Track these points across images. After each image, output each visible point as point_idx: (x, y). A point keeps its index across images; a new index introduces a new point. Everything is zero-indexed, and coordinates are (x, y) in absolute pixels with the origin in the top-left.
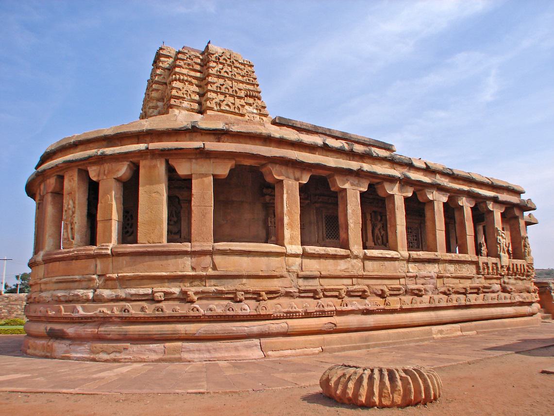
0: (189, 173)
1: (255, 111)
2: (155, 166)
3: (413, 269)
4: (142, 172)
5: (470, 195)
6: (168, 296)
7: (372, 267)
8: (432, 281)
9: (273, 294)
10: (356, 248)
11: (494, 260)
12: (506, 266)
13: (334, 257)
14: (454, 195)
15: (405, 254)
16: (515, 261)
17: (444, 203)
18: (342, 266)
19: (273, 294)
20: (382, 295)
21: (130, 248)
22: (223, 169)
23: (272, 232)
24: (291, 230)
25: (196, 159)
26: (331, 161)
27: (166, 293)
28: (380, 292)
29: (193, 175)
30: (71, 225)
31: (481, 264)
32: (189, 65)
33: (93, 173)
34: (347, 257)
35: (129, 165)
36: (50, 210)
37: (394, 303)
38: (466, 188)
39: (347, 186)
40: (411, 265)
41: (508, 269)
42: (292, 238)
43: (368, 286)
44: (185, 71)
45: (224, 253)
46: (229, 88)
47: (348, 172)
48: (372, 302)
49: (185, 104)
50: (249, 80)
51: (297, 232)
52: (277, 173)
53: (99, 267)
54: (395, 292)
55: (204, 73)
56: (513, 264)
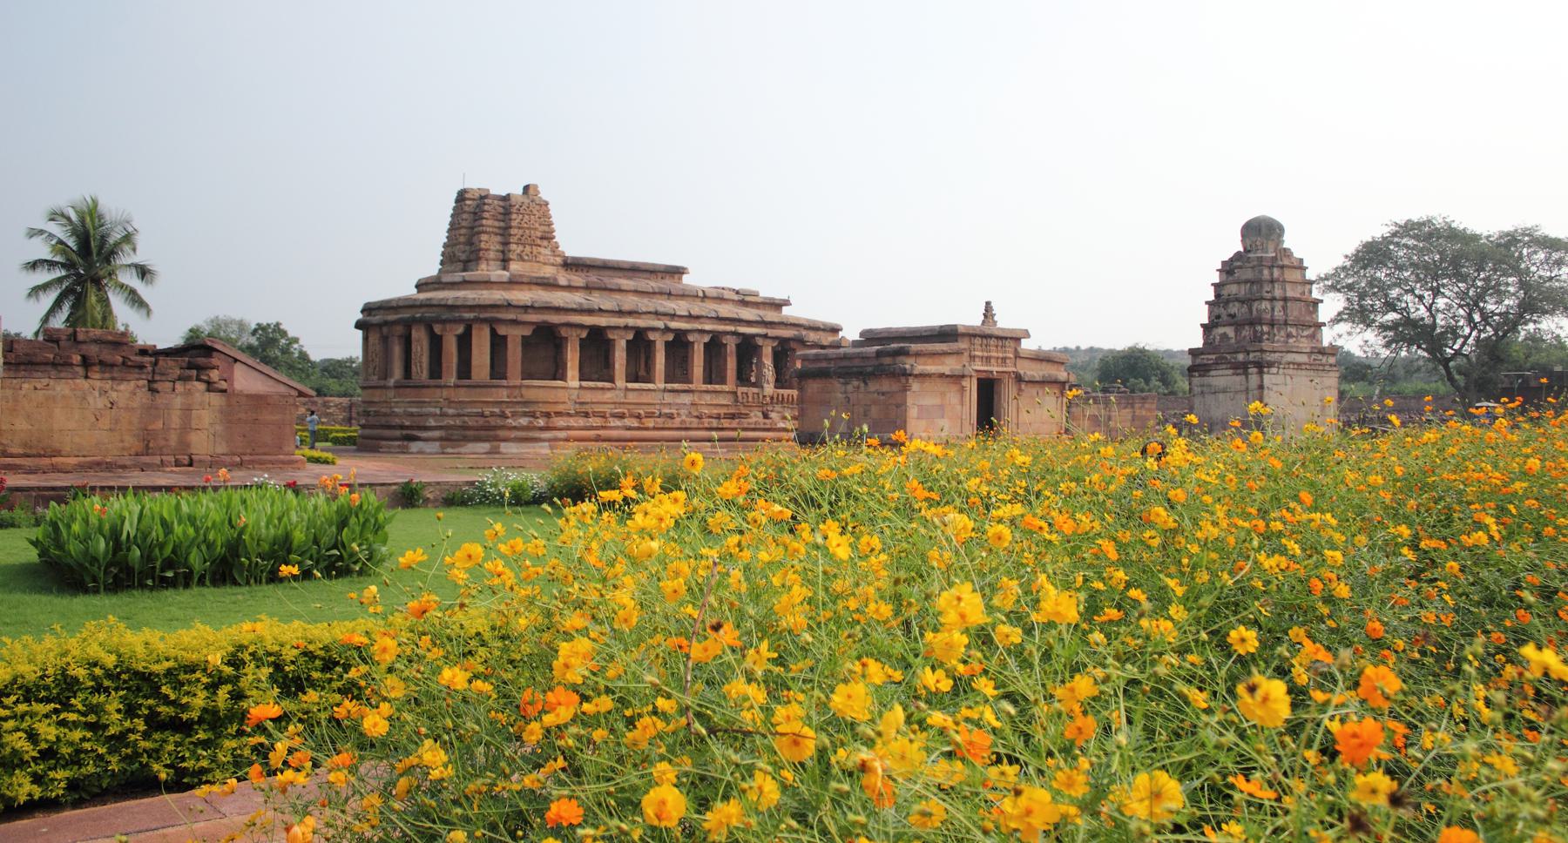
3: (668, 398)
4: (474, 332)
5: (735, 333)
6: (493, 414)
7: (632, 397)
9: (559, 414)
10: (620, 382)
11: (755, 390)
15: (662, 386)
16: (781, 391)
18: (608, 396)
19: (559, 414)
20: (639, 417)
21: (466, 382)
22: (527, 332)
23: (558, 373)
24: (572, 371)
26: (602, 321)
33: (437, 329)
36: (397, 350)
37: (650, 423)
44: (490, 222)
45: (528, 387)
48: (629, 422)
49: (492, 255)
52: (564, 332)
54: (650, 415)
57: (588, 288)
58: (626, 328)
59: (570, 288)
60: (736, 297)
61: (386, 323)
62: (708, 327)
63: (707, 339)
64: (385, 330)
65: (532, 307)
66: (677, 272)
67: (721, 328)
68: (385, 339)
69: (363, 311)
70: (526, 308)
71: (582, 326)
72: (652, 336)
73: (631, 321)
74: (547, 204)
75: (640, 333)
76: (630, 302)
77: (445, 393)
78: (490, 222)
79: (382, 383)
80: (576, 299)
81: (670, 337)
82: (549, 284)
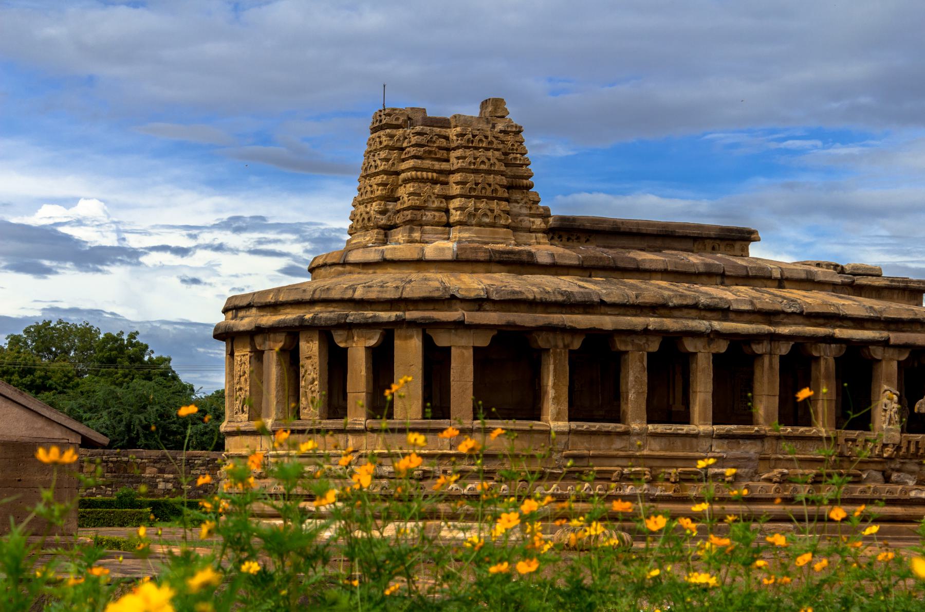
0: (448, 345)
1: (524, 211)
2: (411, 337)
4: (397, 343)
5: (830, 339)
8: (751, 464)
12: (894, 445)
13: (608, 433)
14: (800, 344)
17: (781, 356)
18: (618, 444)
21: (384, 424)
25: (456, 329)
26: (607, 322)
27: (425, 472)
28: (666, 476)
29: (453, 349)
30: (312, 392)
31: (841, 440)
32: (430, 152)
34: (627, 433)
35: (381, 334)
38: (822, 331)
39: (629, 348)
40: (715, 443)
41: (898, 448)
42: (558, 413)
43: (651, 467)
46: (487, 187)
47: (630, 332)
50: (515, 158)
51: (565, 407)
52: (541, 341)
53: (350, 442)
55: (451, 160)
56: (909, 442)
57: (585, 269)
58: (646, 332)
59: (555, 268)
60: (838, 279)
61: (260, 331)
62: (785, 330)
63: (784, 349)
64: (258, 340)
65: (488, 300)
66: (740, 238)
67: (810, 330)
68: (258, 356)
69: (225, 311)
70: (479, 303)
71: (573, 331)
72: (690, 346)
73: (653, 322)
74: (518, 132)
75: (671, 340)
76: (658, 289)
77: (352, 441)
78: (427, 163)
79: (254, 425)
80: (568, 284)
81: (722, 347)
82: (522, 264)
